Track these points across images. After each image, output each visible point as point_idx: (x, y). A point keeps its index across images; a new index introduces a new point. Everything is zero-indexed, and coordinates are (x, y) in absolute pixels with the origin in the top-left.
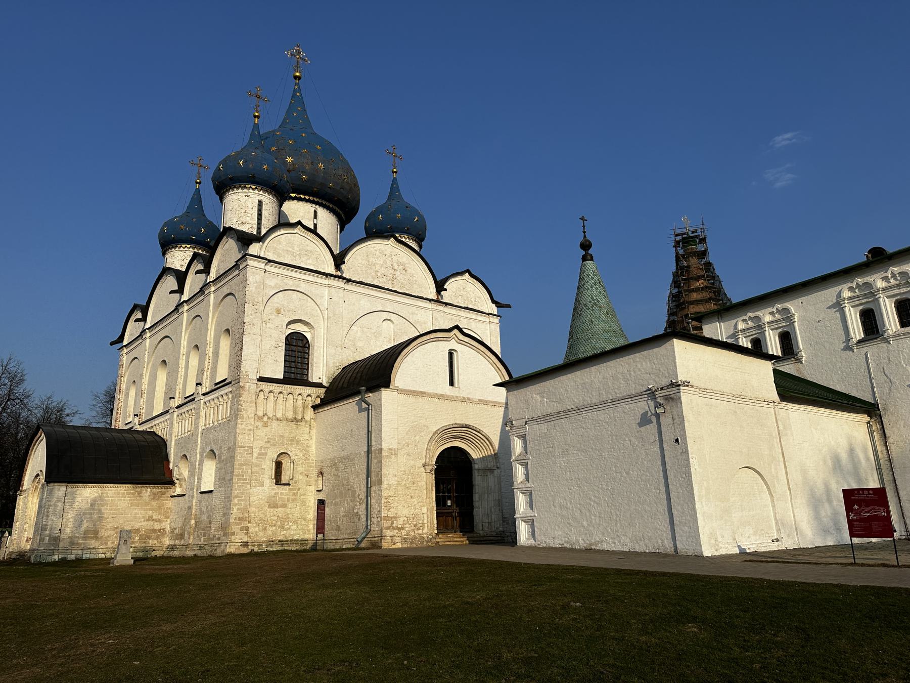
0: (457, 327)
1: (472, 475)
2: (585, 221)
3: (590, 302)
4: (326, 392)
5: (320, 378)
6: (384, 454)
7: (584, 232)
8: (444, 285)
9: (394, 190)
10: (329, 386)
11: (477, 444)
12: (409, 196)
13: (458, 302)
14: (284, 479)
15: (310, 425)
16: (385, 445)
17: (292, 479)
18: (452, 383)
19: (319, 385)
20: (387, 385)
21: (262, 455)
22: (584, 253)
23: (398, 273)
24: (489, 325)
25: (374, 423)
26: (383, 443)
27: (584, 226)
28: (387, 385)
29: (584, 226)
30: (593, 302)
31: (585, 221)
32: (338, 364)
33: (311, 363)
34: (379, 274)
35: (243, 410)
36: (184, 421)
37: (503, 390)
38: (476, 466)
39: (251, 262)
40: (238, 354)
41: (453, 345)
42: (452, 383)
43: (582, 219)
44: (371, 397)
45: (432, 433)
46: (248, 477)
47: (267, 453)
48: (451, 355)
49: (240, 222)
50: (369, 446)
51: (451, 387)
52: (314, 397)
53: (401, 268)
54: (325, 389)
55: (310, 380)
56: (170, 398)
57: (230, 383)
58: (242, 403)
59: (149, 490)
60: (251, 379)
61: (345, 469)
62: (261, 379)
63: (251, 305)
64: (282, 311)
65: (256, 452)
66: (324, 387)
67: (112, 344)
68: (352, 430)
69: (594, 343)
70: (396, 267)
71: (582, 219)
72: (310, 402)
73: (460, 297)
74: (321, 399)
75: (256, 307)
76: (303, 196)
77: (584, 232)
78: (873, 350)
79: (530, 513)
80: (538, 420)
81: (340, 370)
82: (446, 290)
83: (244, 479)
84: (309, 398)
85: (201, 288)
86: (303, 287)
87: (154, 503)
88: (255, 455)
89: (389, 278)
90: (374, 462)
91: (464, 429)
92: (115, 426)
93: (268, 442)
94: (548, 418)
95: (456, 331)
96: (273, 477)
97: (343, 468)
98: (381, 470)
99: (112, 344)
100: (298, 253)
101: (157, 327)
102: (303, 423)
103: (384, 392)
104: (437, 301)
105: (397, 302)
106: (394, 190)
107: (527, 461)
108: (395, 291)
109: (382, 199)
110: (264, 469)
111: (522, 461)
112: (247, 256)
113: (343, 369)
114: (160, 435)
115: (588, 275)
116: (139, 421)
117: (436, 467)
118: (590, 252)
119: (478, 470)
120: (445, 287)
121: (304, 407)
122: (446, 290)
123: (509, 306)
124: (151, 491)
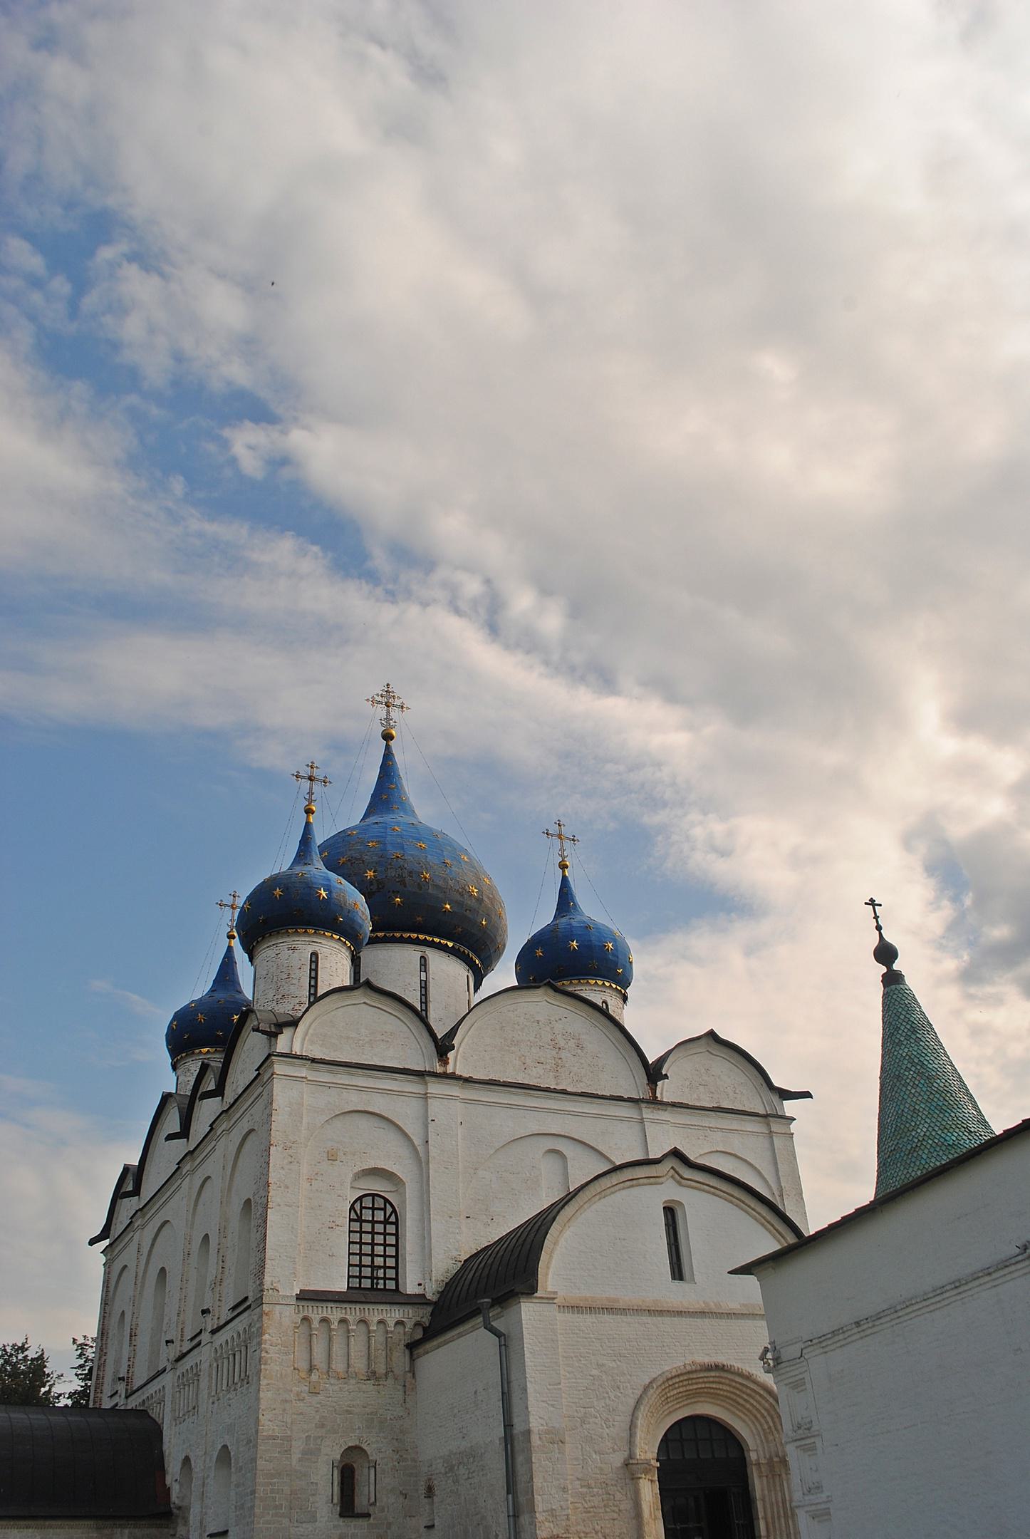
0: (676, 1153)
2: (876, 907)
3: (908, 1069)
5: (420, 1285)
6: (535, 1440)
7: (879, 928)
8: (661, 1068)
9: (565, 900)
10: (439, 1298)
11: (748, 1406)
12: (590, 909)
13: (699, 1099)
14: (361, 1502)
15: (405, 1386)
16: (535, 1424)
17: (374, 1504)
18: (678, 1273)
19: (418, 1301)
21: (310, 1453)
22: (884, 969)
23: (563, 1054)
26: (532, 1419)
27: (876, 917)
29: (876, 917)
30: (913, 1069)
31: (876, 907)
32: (455, 1253)
33: (402, 1256)
34: (528, 1061)
35: (269, 1362)
36: (187, 1388)
37: (751, 1281)
39: (280, 1068)
40: (261, 1246)
41: (669, 1191)
43: (872, 903)
45: (641, 1389)
46: (284, 1503)
47: (320, 1450)
48: (670, 1212)
49: (280, 996)
50: (508, 1426)
52: (409, 1325)
53: (572, 1043)
54: (430, 1309)
56: (167, 1342)
57: (249, 1307)
58: (267, 1346)
59: (126, 1531)
60: (284, 1296)
61: (469, 1478)
62: (306, 1297)
63: (280, 1148)
64: (340, 1154)
65: (298, 1446)
66: (428, 1303)
67: (93, 1242)
68: (476, 1392)
69: (924, 1156)
70: (562, 1043)
71: (872, 903)
72: (400, 1337)
73: (701, 1088)
74: (425, 1329)
75: (291, 1152)
76: (421, 937)
77: (879, 928)
80: (824, 1344)
81: (460, 1265)
82: (666, 1077)
83: (276, 1507)
84: (400, 1329)
85: (211, 1126)
86: (379, 1104)
88: (296, 1456)
89: (548, 1067)
91: (713, 1374)
92: (95, 1402)
93: (323, 1426)
94: (841, 1337)
95: (672, 1162)
96: (335, 1501)
97: (466, 1476)
98: (532, 1478)
99: (93, 1242)
100: (367, 1039)
101: (154, 1205)
102: (390, 1381)
104: (654, 1101)
105: (569, 1113)
106: (565, 900)
107: (812, 1440)
108: (564, 1092)
109: (545, 917)
110: (316, 1484)
111: (803, 1442)
112: (273, 1058)
113: (465, 1261)
114: (153, 1416)
116: (127, 1390)
117: (658, 1465)
118: (896, 966)
120: (664, 1072)
121: (389, 1349)
122: (666, 1077)
123: (807, 1095)
124: (130, 1533)
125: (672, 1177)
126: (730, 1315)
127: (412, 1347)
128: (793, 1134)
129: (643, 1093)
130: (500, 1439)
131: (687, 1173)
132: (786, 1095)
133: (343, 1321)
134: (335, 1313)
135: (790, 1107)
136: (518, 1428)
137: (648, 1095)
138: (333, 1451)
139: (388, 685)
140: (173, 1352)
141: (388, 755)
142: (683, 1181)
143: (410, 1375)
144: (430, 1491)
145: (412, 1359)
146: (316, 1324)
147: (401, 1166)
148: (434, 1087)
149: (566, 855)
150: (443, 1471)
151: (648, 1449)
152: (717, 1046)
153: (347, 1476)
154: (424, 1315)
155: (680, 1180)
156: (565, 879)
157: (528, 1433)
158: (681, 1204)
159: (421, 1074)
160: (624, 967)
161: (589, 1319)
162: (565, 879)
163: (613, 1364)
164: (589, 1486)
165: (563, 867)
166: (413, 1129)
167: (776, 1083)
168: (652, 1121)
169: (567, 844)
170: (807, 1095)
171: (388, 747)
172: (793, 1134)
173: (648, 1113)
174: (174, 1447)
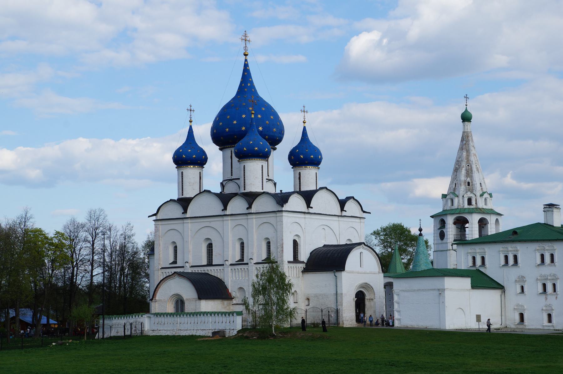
1: (365, 301)
4: (306, 265)
6: (343, 295)
7: (420, 225)
19: (303, 262)
24: (360, 223)
25: (338, 284)
28: (344, 270)
38: (367, 298)
43: (420, 220)
44: (338, 274)
54: (305, 264)
55: (299, 259)
59: (226, 302)
66: (305, 263)
68: (326, 284)
71: (420, 220)
74: (304, 268)
77: (420, 225)
78: (506, 269)
79: (399, 317)
87: (228, 307)
90: (339, 298)
95: (363, 245)
103: (343, 274)
115: (421, 242)
119: (367, 299)
123: (370, 213)
126: (368, 273)
127: (302, 272)
129: (339, 214)
130: (334, 294)
132: (364, 212)
133: (293, 267)
135: (365, 215)
136: (339, 292)
137: (340, 215)
139: (245, 31)
140: (228, 263)
144: (308, 299)
150: (314, 296)
154: (303, 266)
156: (305, 128)
157: (342, 294)
158: (362, 252)
159: (304, 213)
162: (305, 128)
167: (364, 210)
168: (341, 221)
169: (305, 113)
170: (370, 213)
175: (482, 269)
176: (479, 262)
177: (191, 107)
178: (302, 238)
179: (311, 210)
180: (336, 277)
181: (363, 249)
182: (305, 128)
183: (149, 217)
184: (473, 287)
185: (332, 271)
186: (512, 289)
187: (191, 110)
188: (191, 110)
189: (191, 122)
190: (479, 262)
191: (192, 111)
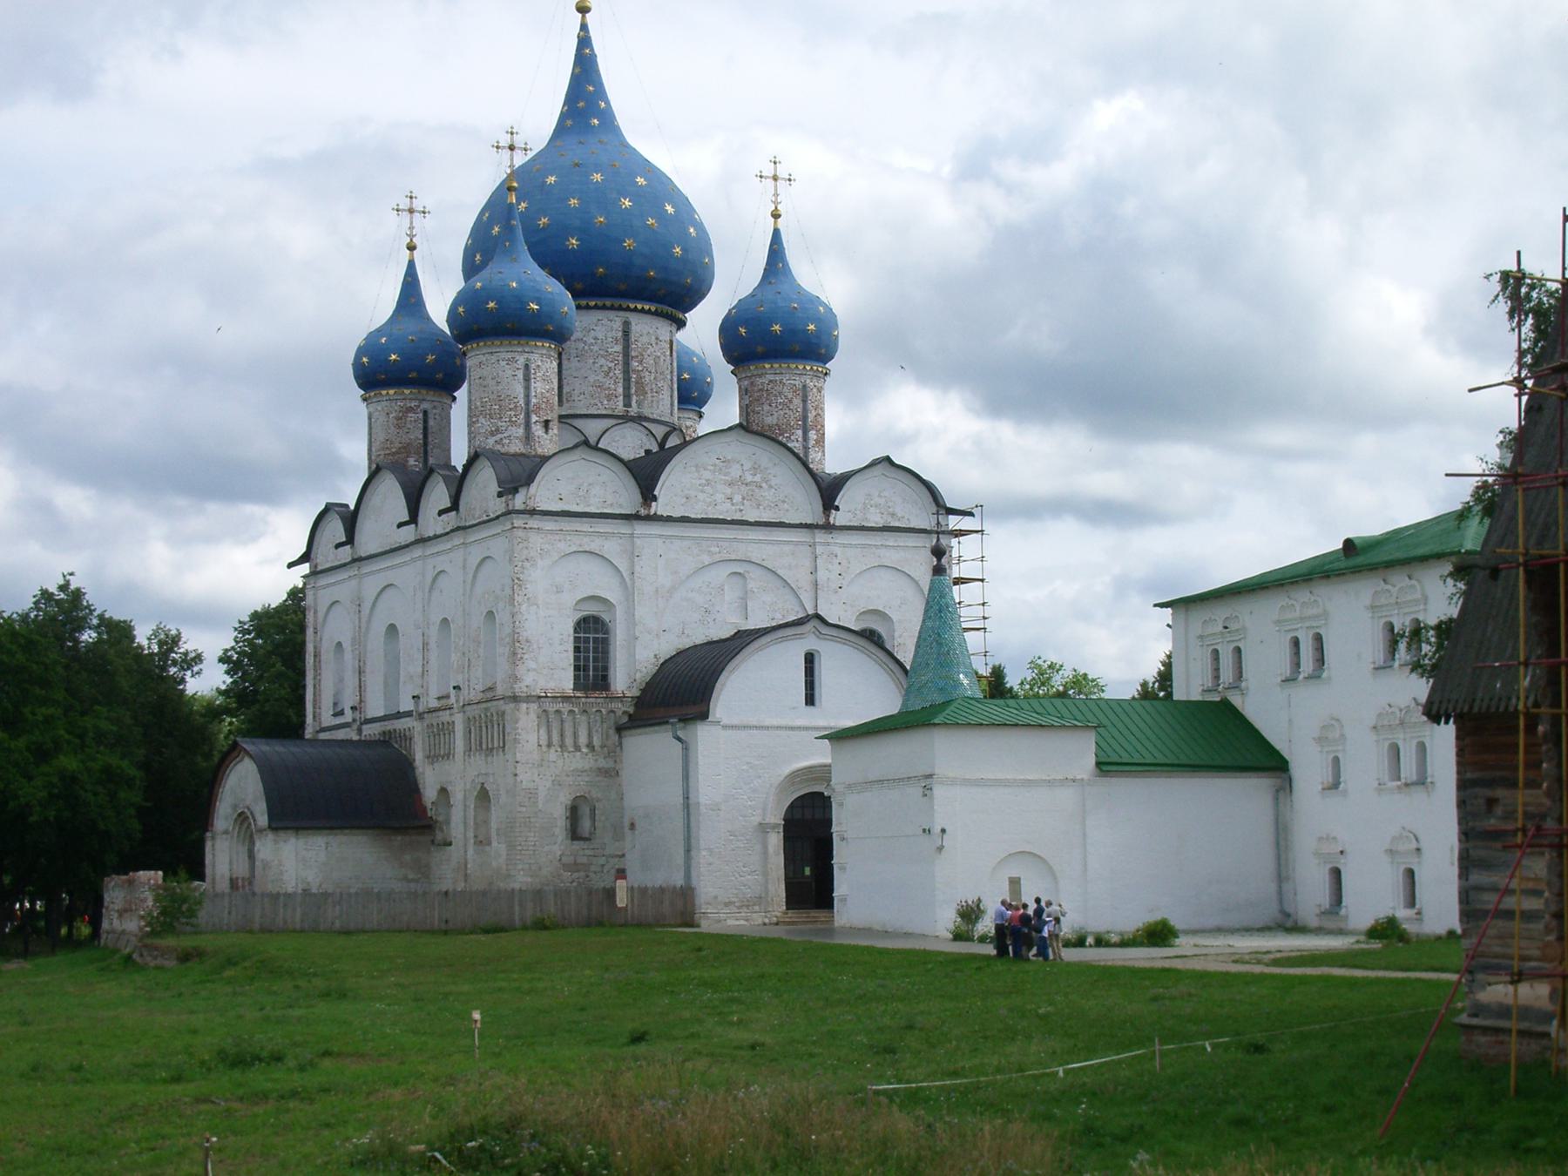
16: (703, 800)
18: (810, 700)
20: (704, 716)
28: (704, 716)
42: (810, 700)
48: (810, 659)
51: (810, 708)
52: (619, 713)
74: (630, 716)
86: (594, 545)
104: (828, 527)
125: (814, 632)
128: (952, 547)
131: (825, 630)
134: (565, 708)
138: (565, 798)
141: (584, 41)
142: (821, 636)
143: (618, 748)
144: (632, 826)
145: (620, 737)
146: (552, 716)
147: (613, 595)
148: (640, 529)
149: (779, 201)
151: (776, 817)
152: (893, 469)
153: (574, 812)
155: (819, 635)
156: (776, 233)
158: (818, 652)
160: (827, 346)
161: (743, 734)
162: (776, 233)
163: (757, 763)
164: (735, 836)
165: (776, 216)
166: (623, 566)
171: (584, 27)
172: (952, 547)
173: (820, 537)
174: (430, 779)
175: (1236, 700)
176: (1227, 675)
177: (411, 203)
178: (620, 613)
179: (658, 508)
180: (679, 739)
181: (818, 637)
182: (776, 234)
183: (290, 565)
184: (1105, 768)
185: (667, 722)
186: (1308, 769)
187: (411, 211)
188: (411, 211)
189: (411, 248)
190: (1227, 675)
191: (416, 214)
